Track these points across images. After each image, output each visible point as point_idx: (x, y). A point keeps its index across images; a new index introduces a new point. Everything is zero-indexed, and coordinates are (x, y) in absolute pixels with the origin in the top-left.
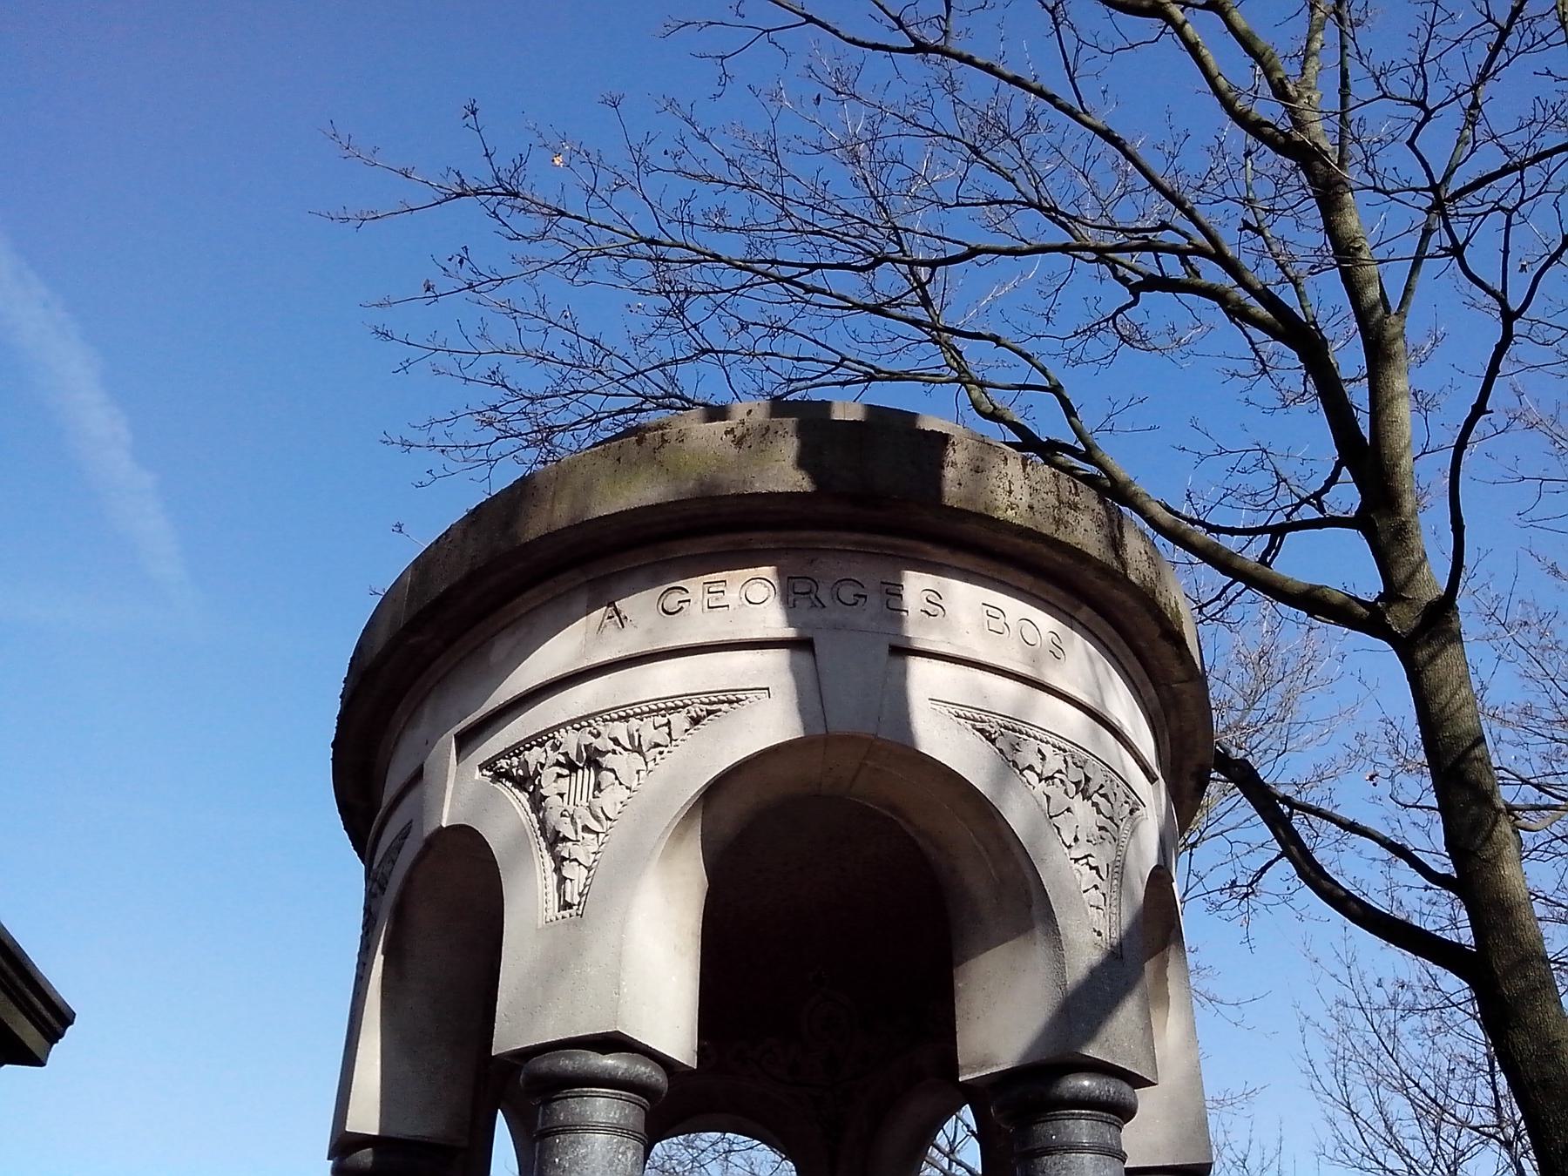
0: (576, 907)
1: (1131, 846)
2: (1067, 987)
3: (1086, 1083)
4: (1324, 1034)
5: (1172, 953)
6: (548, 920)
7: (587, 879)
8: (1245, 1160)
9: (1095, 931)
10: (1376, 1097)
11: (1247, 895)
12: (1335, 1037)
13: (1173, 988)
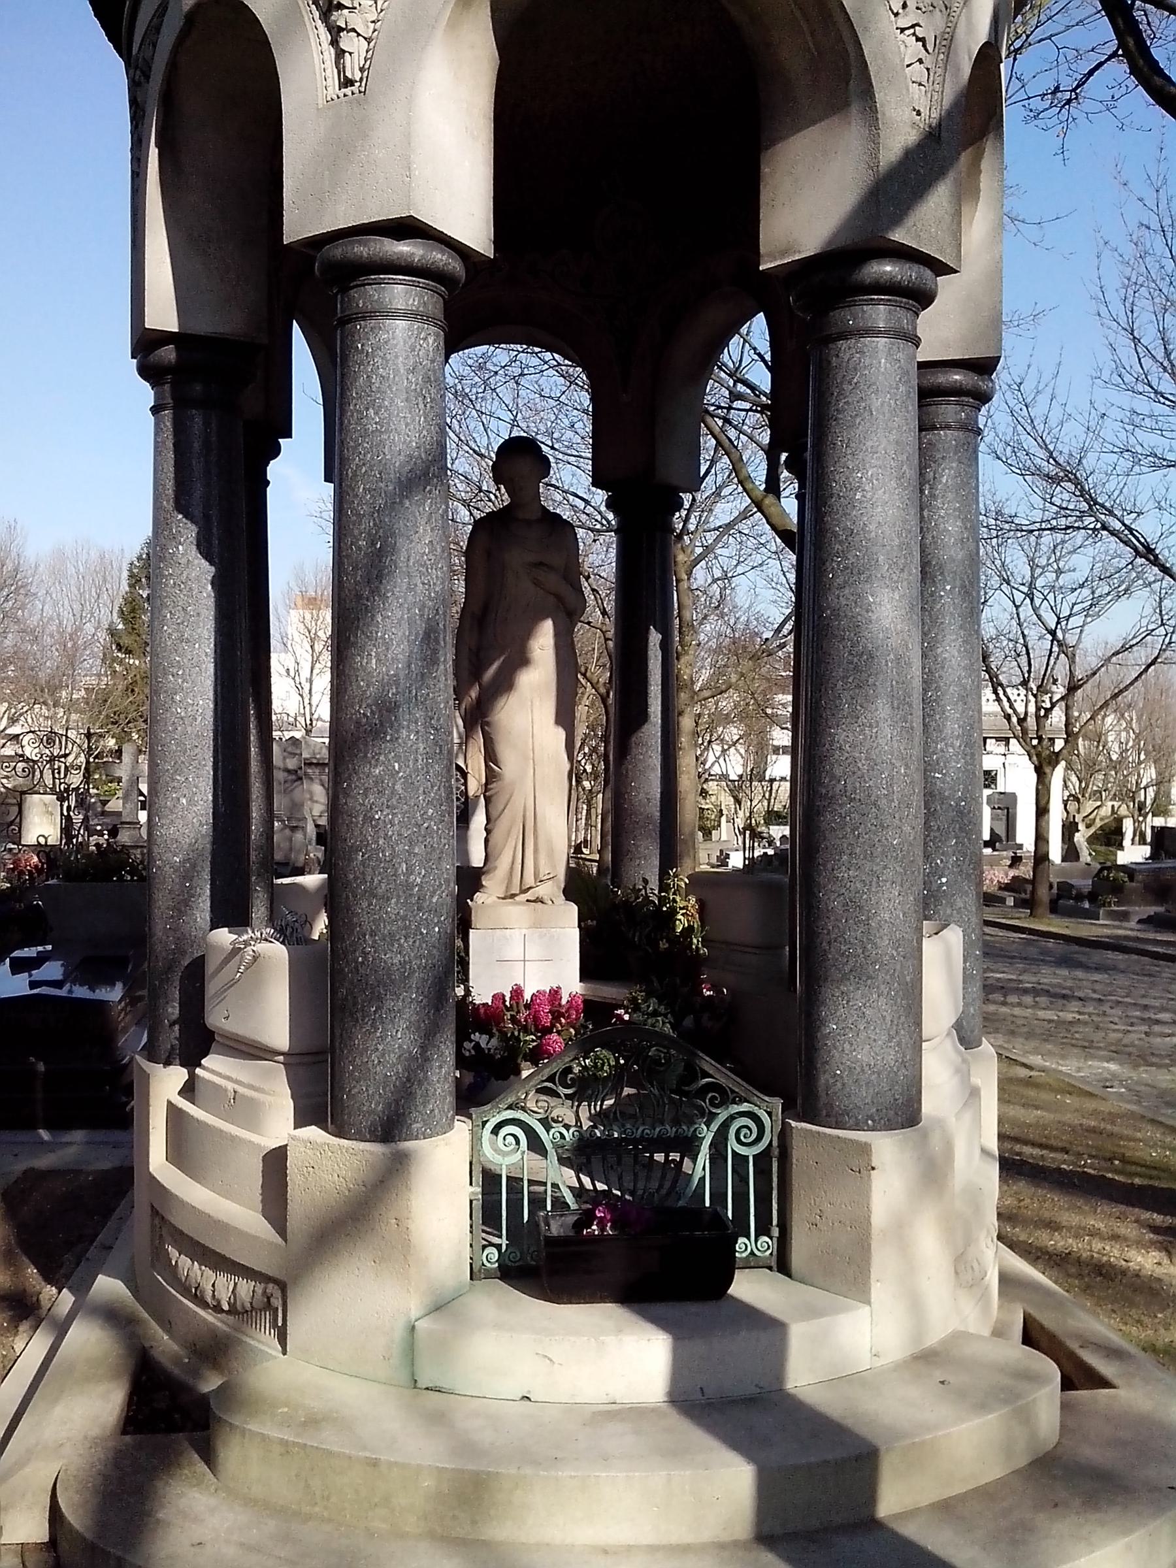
0: (358, 84)
1: (963, 18)
2: (880, 168)
3: (888, 268)
4: (1121, 259)
5: (989, 145)
6: (329, 99)
7: (367, 52)
8: (1021, 384)
9: (914, 110)
10: (1161, 323)
11: (1069, 102)
12: (1131, 263)
13: (986, 181)
